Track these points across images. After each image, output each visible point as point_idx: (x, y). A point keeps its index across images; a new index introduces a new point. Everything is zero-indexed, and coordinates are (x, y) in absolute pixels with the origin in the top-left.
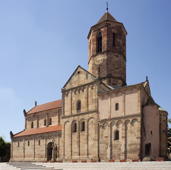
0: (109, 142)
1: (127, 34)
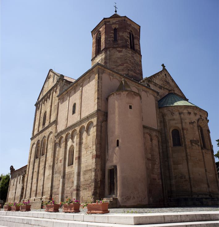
0: (62, 169)
1: (140, 26)
